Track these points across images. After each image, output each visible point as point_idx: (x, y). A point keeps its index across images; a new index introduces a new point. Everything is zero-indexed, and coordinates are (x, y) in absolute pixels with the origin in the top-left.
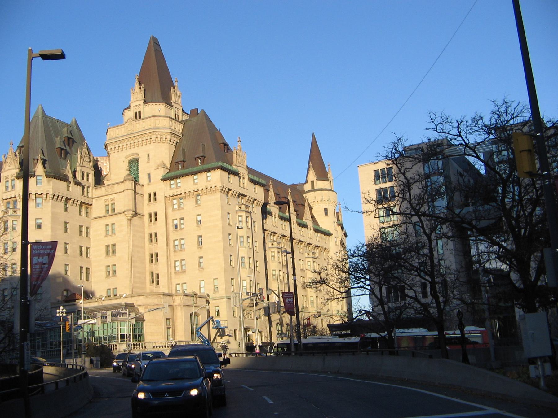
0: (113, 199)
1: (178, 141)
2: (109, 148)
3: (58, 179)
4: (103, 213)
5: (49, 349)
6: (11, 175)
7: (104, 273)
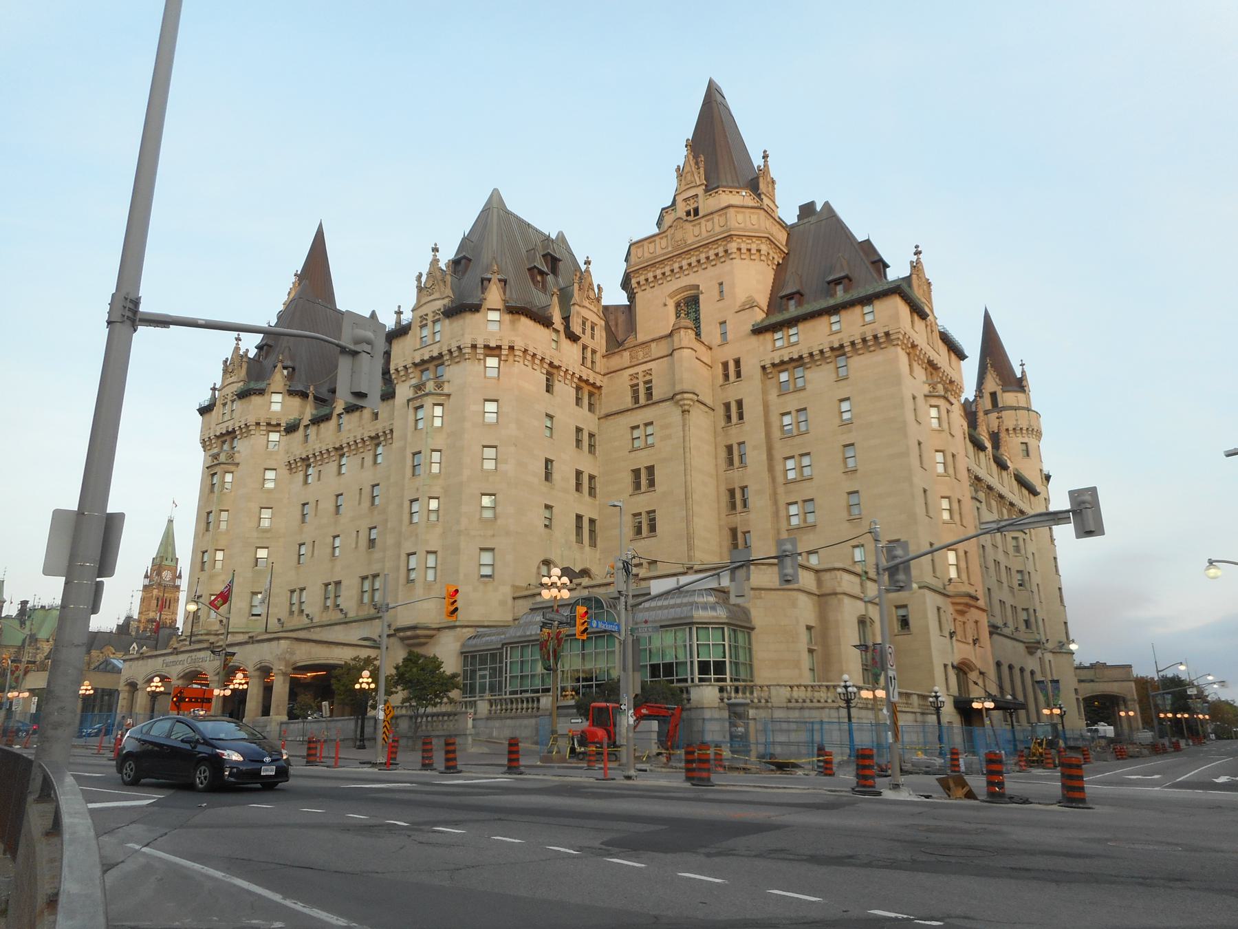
0: (648, 372)
1: (781, 262)
2: (634, 281)
3: (535, 320)
4: (628, 401)
5: (508, 696)
6: (433, 312)
7: (629, 531)
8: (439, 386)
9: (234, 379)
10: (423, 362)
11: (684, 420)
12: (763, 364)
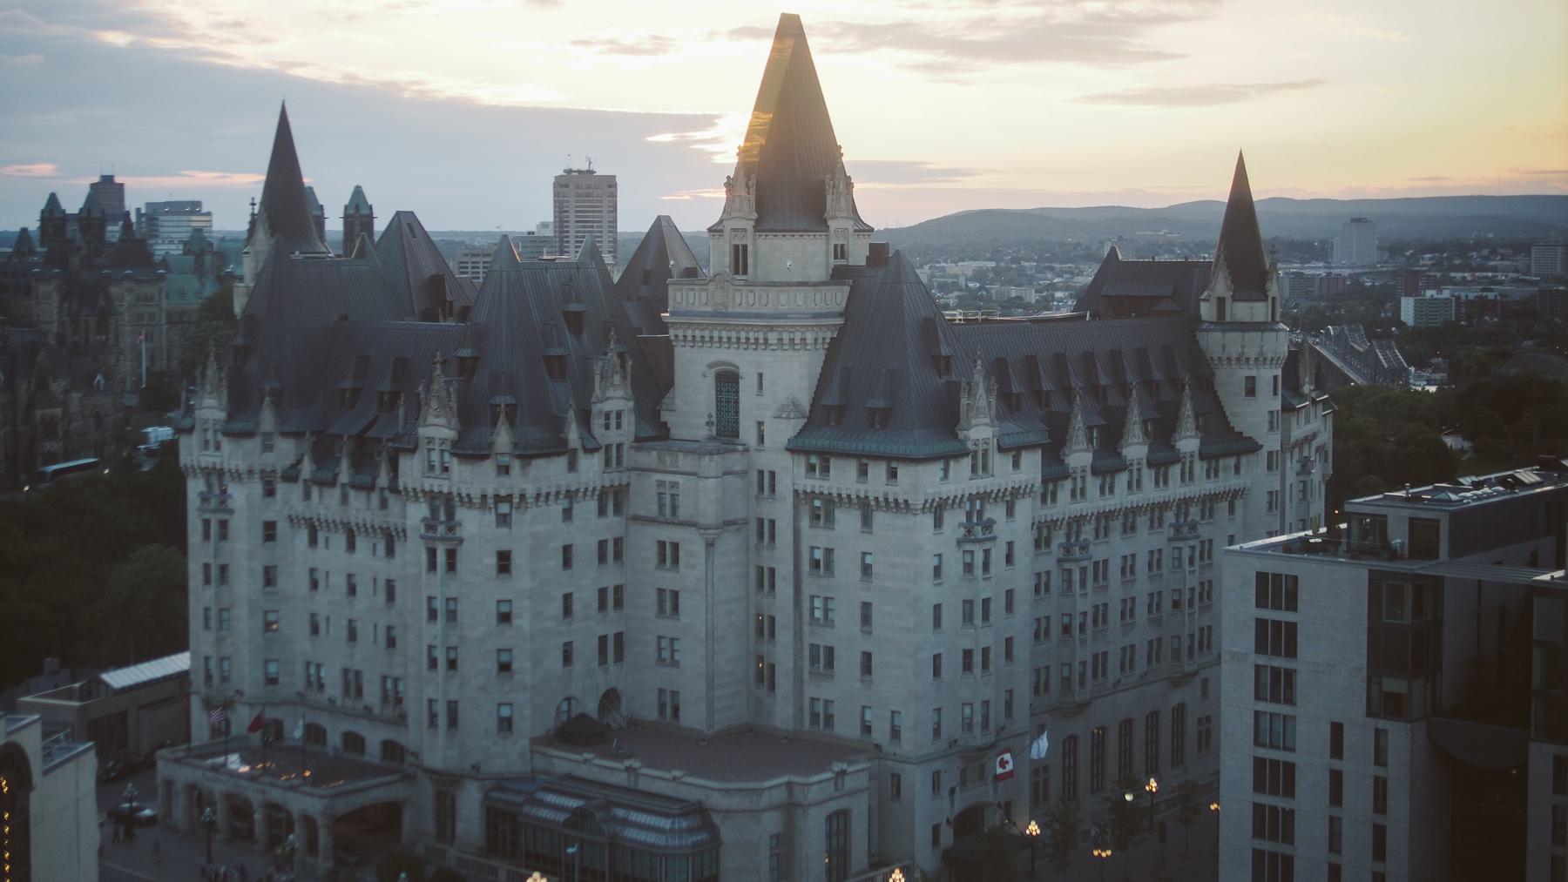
8: (451, 529)
11: (708, 553)
12: (796, 487)
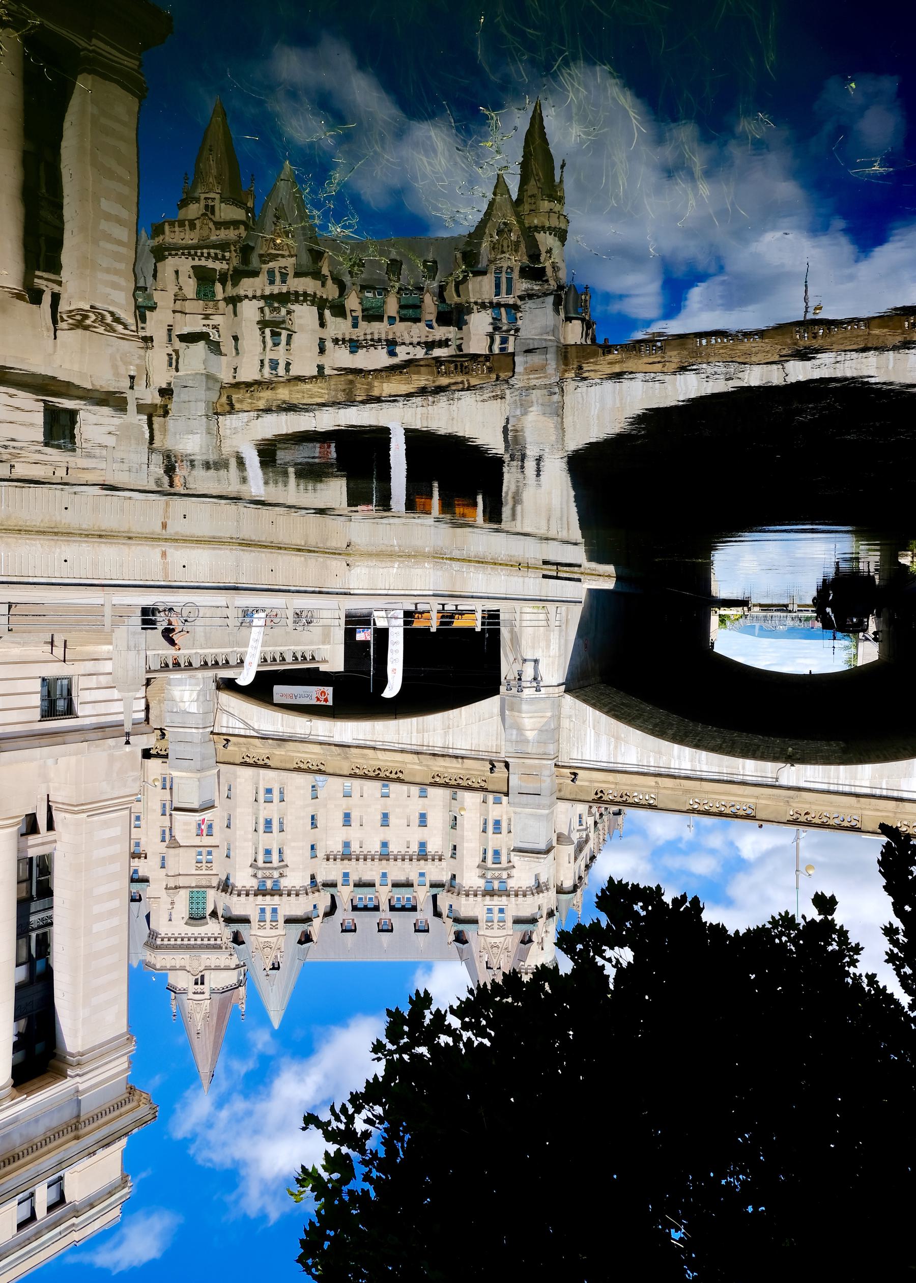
0: (198, 868)
9: (493, 940)
10: (272, 895)
12: (146, 860)
